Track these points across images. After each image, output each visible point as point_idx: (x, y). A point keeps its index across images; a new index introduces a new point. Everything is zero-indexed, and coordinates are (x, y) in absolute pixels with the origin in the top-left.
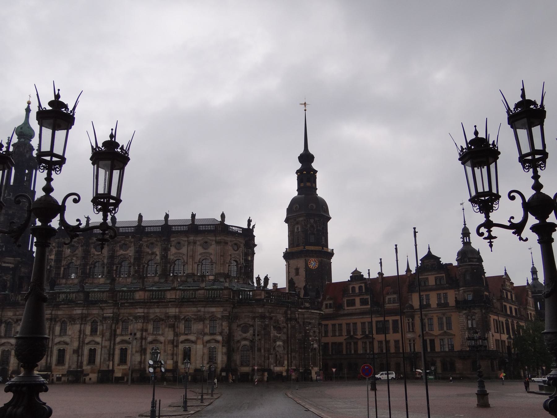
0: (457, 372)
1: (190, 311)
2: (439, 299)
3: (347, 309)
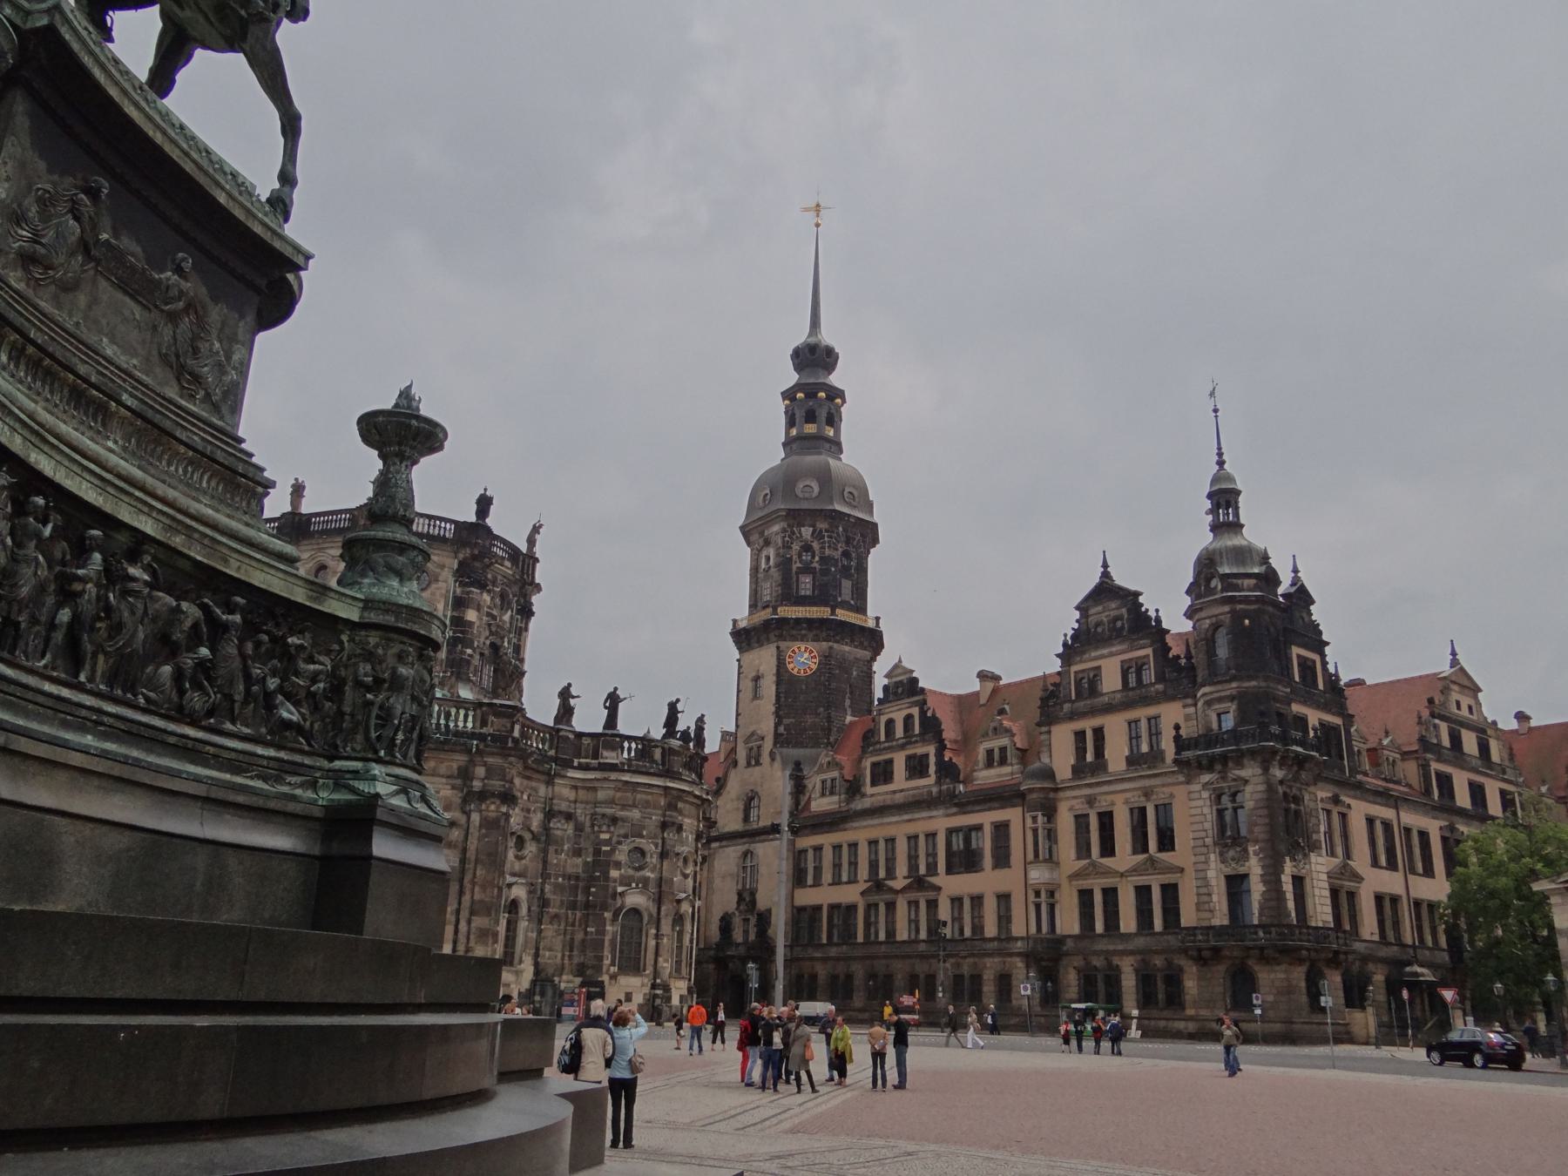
0: (1190, 1012)
2: (1134, 738)
3: (874, 794)
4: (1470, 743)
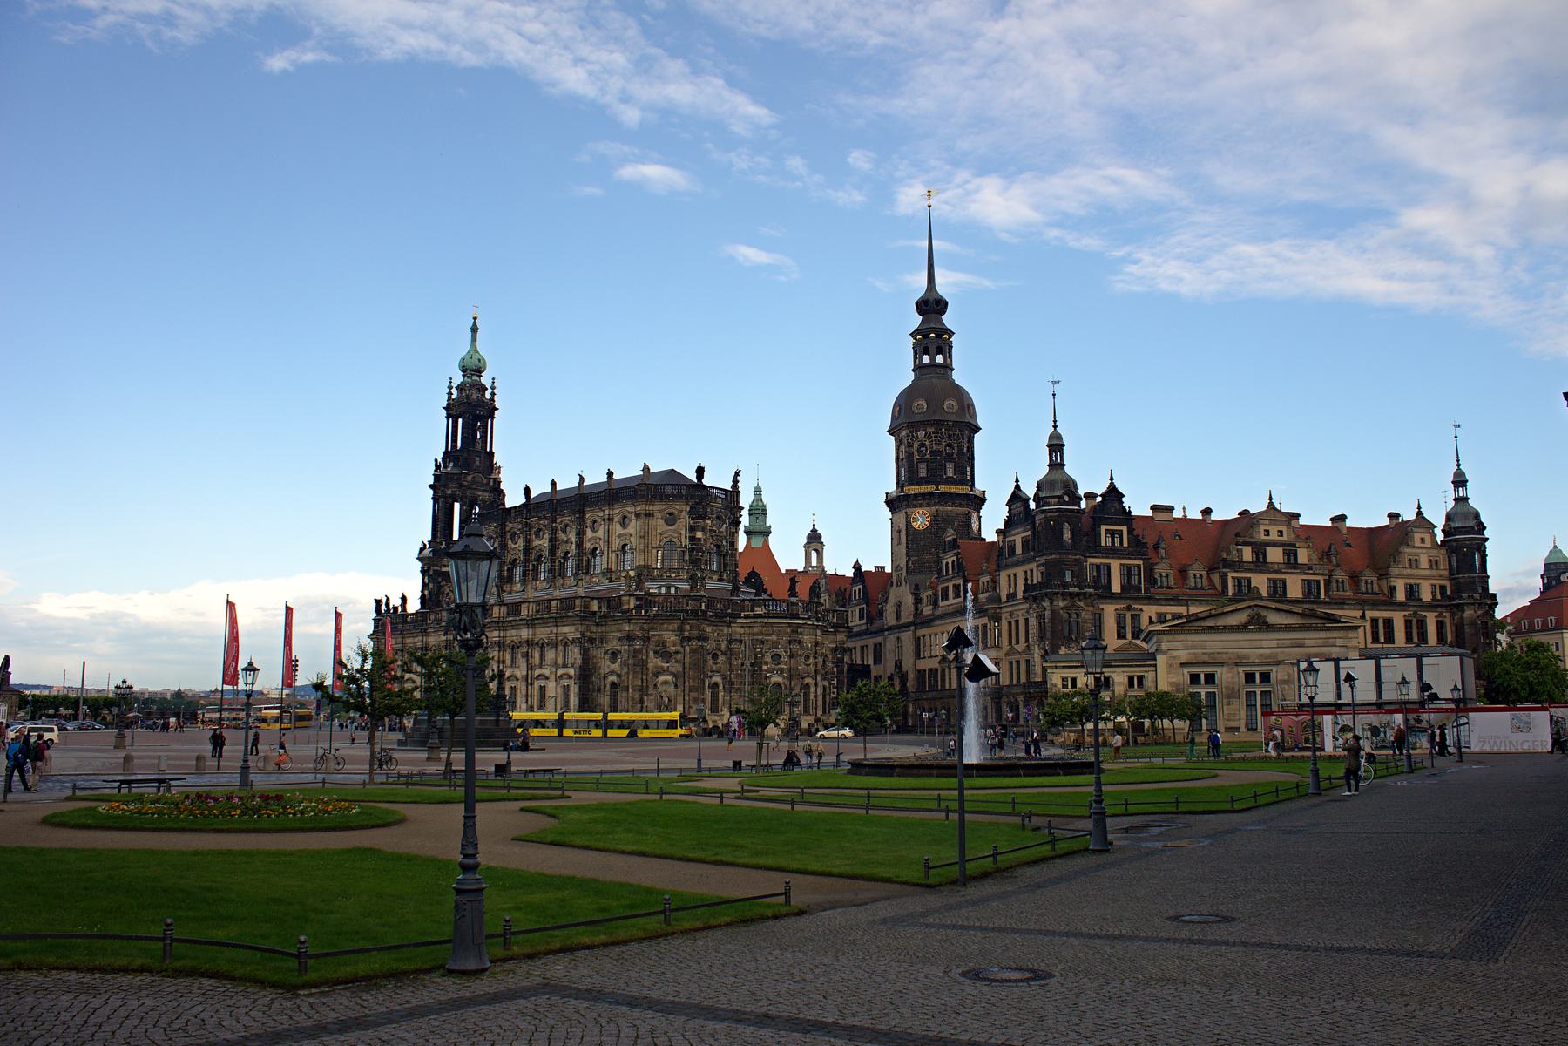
1: (543, 633)
4: (1275, 555)
